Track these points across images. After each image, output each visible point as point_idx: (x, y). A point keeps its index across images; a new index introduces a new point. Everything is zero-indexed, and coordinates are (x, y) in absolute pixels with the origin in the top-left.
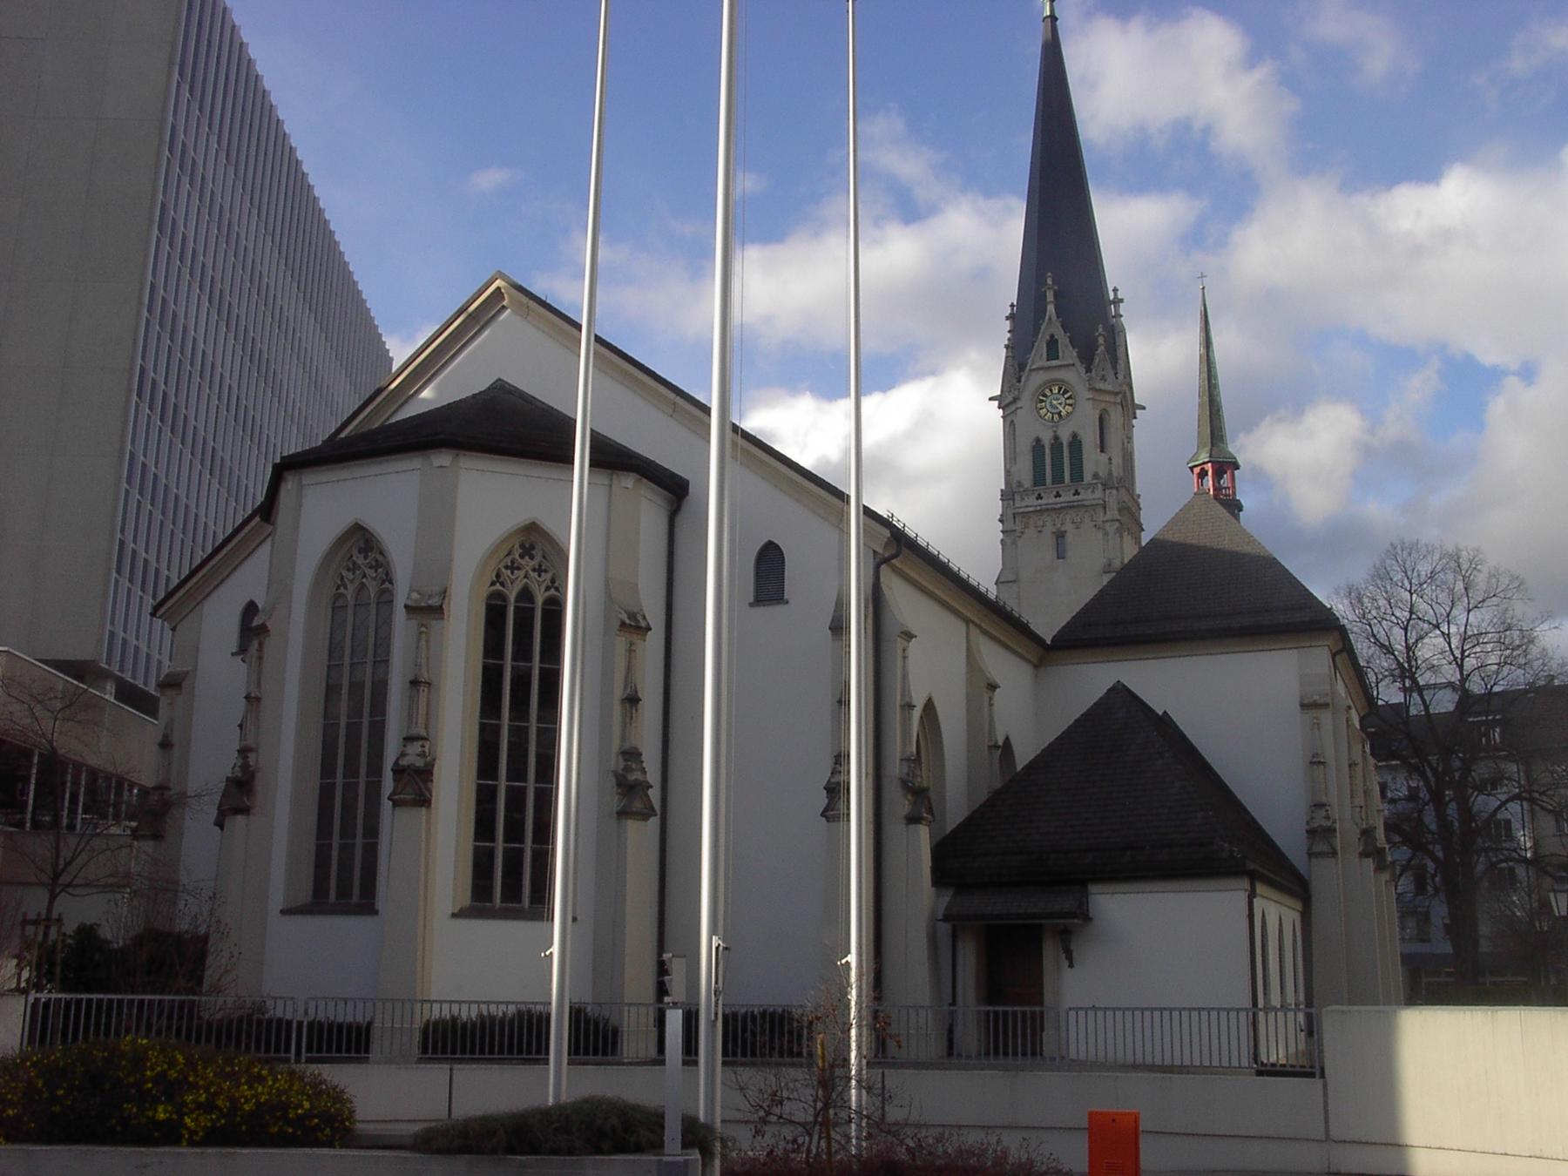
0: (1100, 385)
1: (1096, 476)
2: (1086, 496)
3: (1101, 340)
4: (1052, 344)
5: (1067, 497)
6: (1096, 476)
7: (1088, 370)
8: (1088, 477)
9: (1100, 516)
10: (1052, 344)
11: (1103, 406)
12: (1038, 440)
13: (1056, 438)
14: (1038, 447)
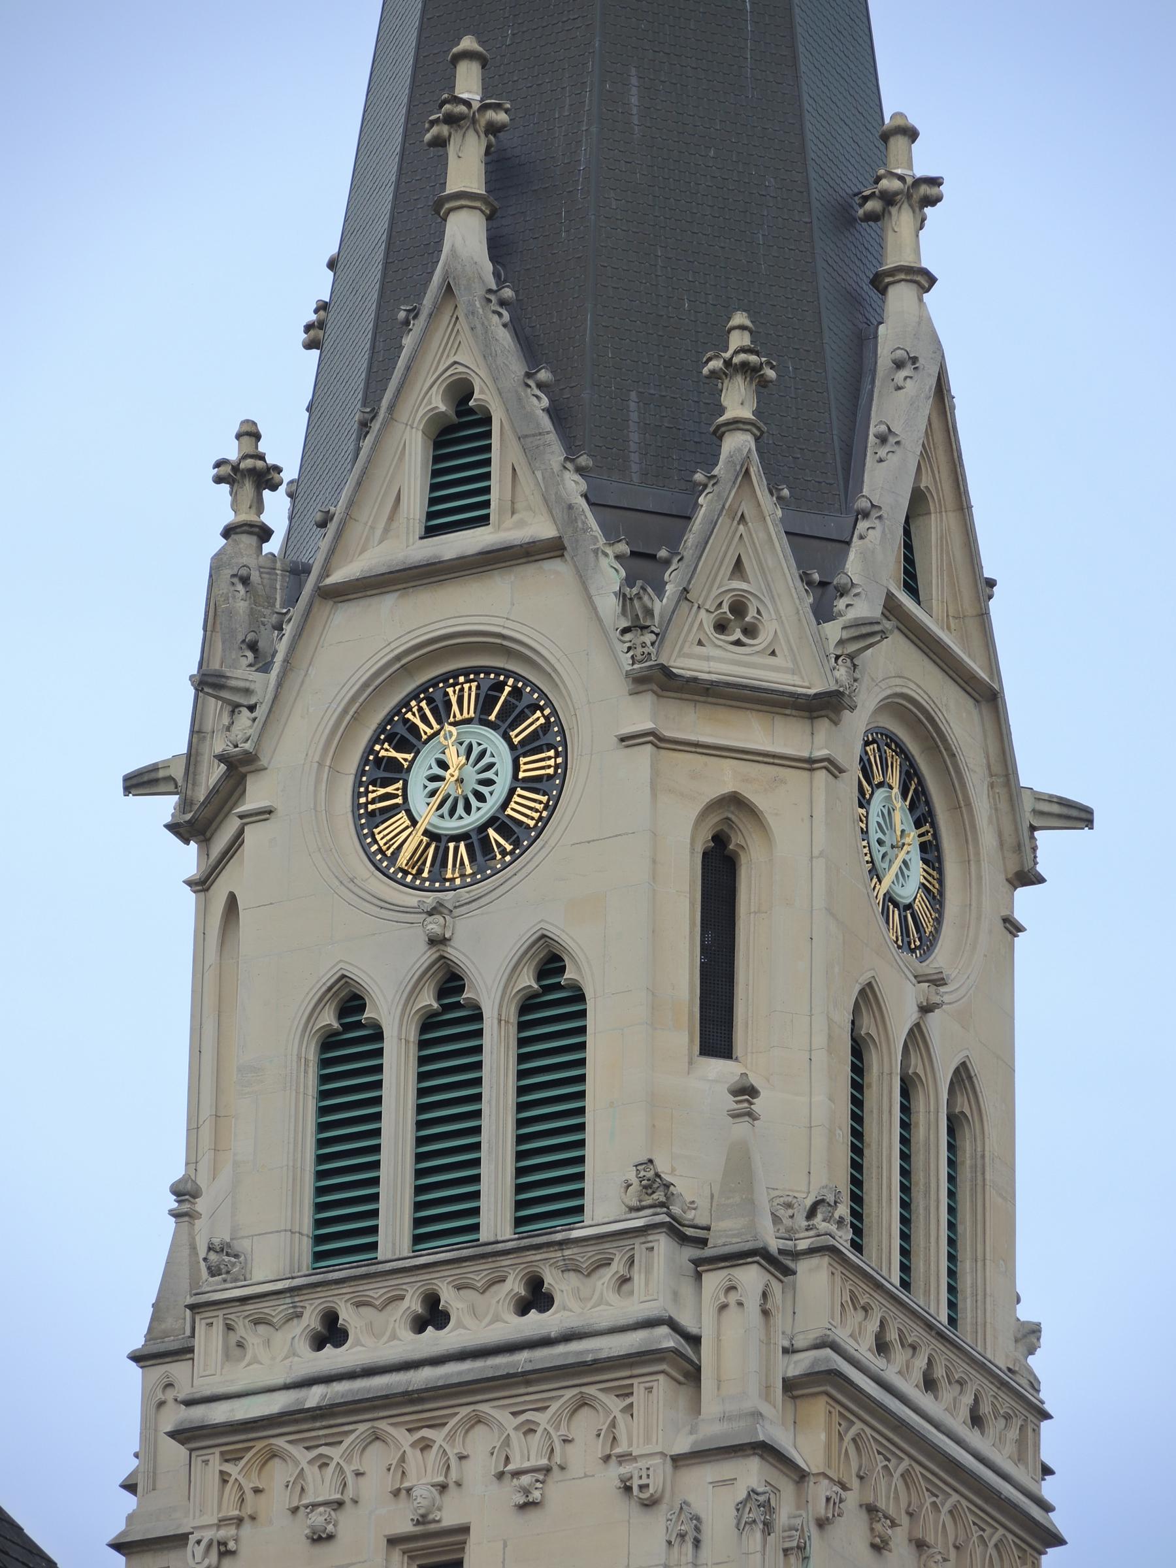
0: (707, 658)
1: (653, 1185)
2: (585, 1303)
3: (738, 401)
4: (460, 437)
5: (483, 1316)
6: (653, 1185)
7: (644, 566)
8: (605, 1201)
9: (655, 1421)
10: (460, 437)
11: (727, 778)
12: (351, 1002)
13: (451, 982)
14: (346, 1041)
